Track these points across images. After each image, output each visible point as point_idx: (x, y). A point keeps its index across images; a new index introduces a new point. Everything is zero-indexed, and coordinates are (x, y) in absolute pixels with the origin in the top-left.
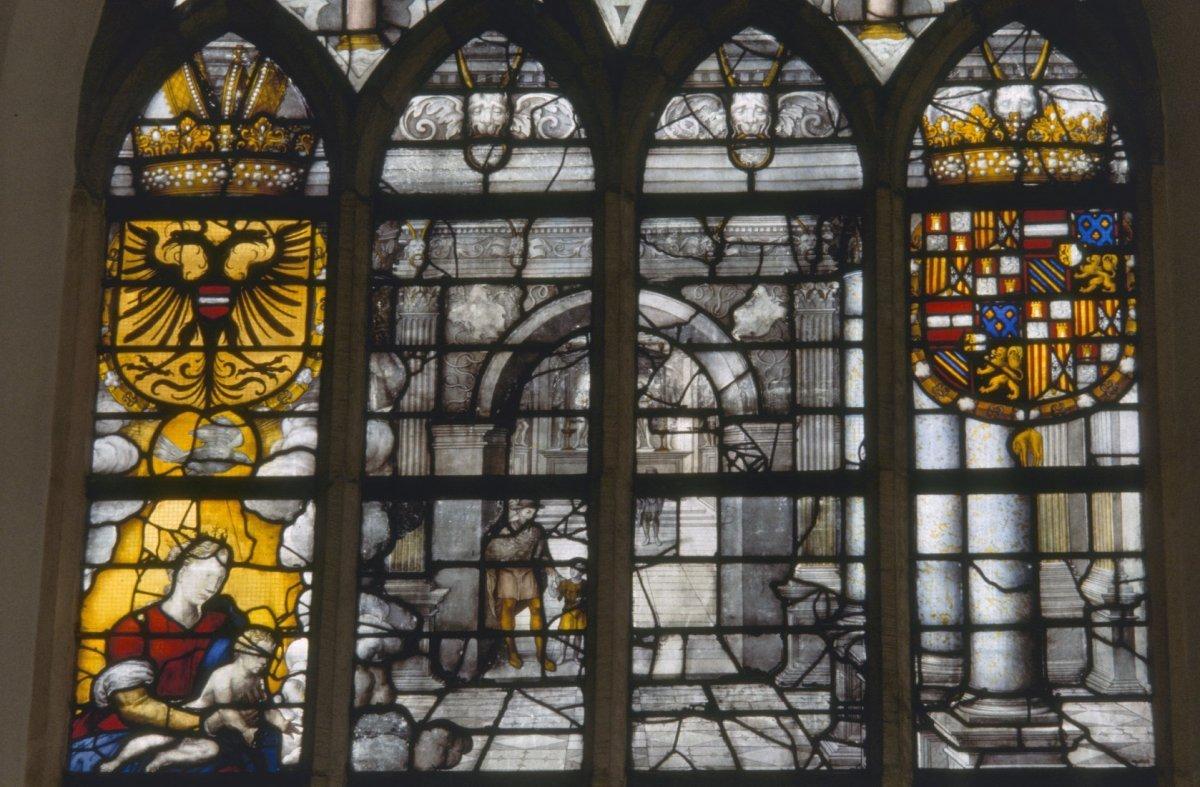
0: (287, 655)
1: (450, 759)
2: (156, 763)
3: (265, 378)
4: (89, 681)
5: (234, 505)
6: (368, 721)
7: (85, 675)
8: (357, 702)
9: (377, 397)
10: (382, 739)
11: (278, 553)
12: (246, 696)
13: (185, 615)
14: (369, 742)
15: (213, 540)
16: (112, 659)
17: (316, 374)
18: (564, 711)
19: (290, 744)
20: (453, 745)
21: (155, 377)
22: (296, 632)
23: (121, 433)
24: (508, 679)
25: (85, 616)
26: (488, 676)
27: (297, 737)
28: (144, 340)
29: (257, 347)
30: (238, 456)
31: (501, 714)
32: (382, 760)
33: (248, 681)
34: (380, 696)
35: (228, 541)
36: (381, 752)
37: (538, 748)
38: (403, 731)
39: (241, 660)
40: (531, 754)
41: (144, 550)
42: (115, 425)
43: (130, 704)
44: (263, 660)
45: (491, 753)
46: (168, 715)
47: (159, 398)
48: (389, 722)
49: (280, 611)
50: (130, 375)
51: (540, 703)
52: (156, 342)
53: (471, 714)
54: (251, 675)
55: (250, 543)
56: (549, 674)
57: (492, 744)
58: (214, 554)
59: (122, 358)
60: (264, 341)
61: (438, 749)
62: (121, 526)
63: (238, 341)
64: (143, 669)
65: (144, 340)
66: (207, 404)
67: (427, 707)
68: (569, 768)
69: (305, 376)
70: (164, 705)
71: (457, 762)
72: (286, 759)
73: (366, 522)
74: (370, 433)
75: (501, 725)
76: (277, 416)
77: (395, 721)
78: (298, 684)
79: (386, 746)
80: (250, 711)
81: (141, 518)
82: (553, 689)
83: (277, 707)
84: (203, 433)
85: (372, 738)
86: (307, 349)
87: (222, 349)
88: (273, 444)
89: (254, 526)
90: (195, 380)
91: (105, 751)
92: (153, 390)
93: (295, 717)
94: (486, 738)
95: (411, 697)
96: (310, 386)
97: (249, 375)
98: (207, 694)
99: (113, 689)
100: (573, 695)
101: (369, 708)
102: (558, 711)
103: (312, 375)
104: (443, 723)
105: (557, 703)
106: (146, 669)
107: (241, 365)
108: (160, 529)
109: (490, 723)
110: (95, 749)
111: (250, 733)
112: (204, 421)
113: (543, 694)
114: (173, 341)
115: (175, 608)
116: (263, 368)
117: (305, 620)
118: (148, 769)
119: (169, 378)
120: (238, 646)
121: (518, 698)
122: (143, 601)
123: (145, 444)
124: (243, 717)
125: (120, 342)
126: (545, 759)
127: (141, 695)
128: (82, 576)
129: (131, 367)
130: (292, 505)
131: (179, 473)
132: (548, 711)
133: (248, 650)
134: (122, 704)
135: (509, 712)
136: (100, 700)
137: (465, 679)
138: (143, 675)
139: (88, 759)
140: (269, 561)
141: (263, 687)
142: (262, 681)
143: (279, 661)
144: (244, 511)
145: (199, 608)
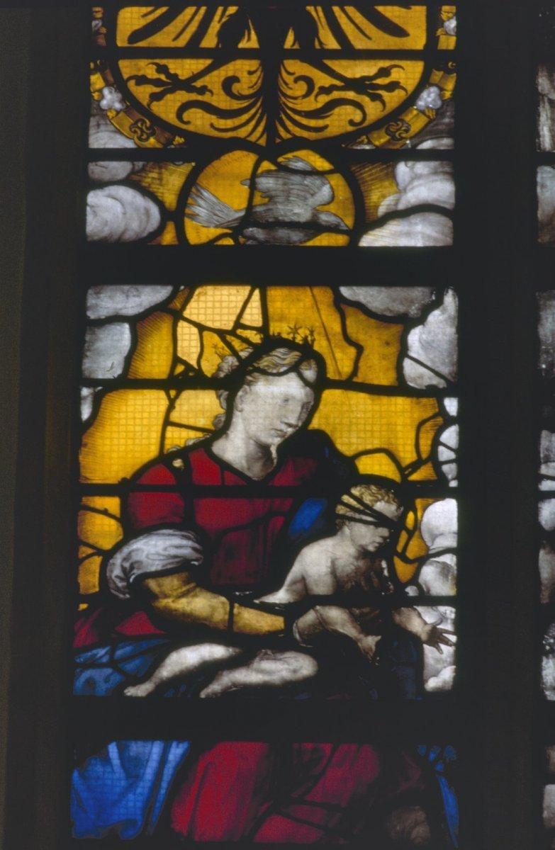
0: (423, 527)
2: (215, 687)
3: (365, 100)
4: (97, 560)
5: (323, 295)
7: (90, 551)
9: (551, 131)
11: (399, 369)
12: (358, 584)
13: (250, 459)
15: (290, 345)
16: (132, 527)
17: (448, 94)
19: (438, 661)
21: (182, 97)
22: (437, 490)
23: (131, 182)
25: (85, 460)
27: (448, 651)
28: (162, 39)
29: (348, 52)
30: (324, 218)
33: (361, 563)
35: (316, 347)
39: (346, 530)
41: (176, 360)
42: (121, 168)
43: (166, 596)
44: (384, 532)
46: (231, 614)
47: (191, 128)
49: (408, 456)
50: (142, 93)
52: (182, 42)
54: (363, 553)
55: (352, 351)
58: (295, 368)
59: (127, 68)
60: (359, 43)
62: (139, 323)
63: (317, 43)
64: (185, 542)
65: (162, 39)
66: (270, 140)
69: (429, 98)
70: (223, 599)
72: (432, 684)
73: (544, 321)
74: (543, 186)
76: (388, 158)
78: (445, 568)
80: (366, 610)
81: (171, 311)
83: (412, 603)
84: (266, 183)
86: (431, 57)
87: (292, 54)
88: (382, 200)
89: (356, 325)
90: (245, 104)
91: (130, 666)
92: (179, 115)
93: (443, 619)
96: (440, 112)
97: (336, 95)
98: (294, 583)
99: (136, 572)
103: (441, 96)
106: (190, 543)
107: (323, 80)
108: (201, 328)
110: (113, 663)
111: (370, 641)
112: (266, 165)
114: (210, 41)
115: (234, 449)
116: (361, 85)
117: (450, 470)
118: (203, 695)
119: (206, 98)
120: (341, 510)
122: (178, 438)
123: (170, 199)
124: (355, 619)
125: (122, 41)
127: (186, 582)
128: (78, 400)
129: (141, 80)
130: (418, 294)
131: (229, 242)
133: (357, 516)
134: (155, 597)
136: (118, 589)
138: (187, 552)
139: (102, 678)
140: (385, 378)
141: (386, 573)
142: (384, 564)
143: (411, 534)
144: (340, 304)
145: (273, 450)
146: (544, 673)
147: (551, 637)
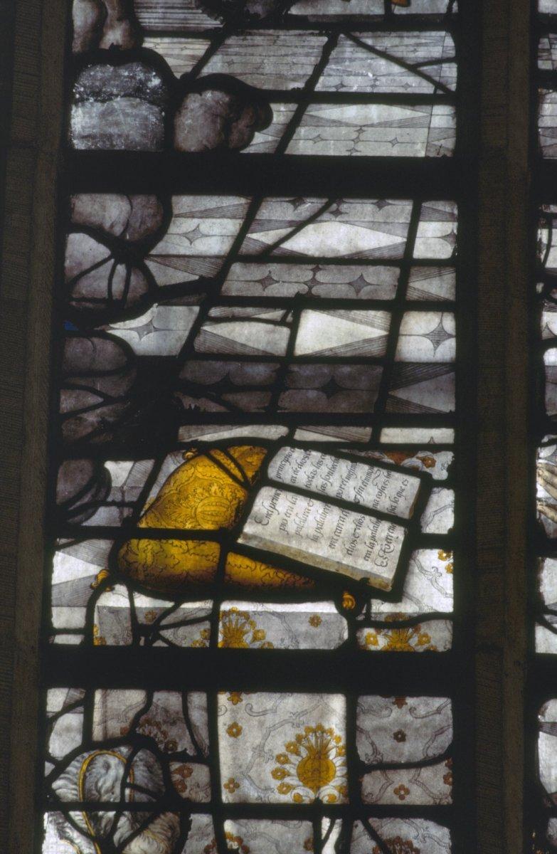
1: (235, 136)
6: (98, 74)
8: (77, 46)
10: (119, 103)
14: (99, 107)
18: (425, 69)
20: (238, 119)
24: (327, 16)
26: (294, 11)
31: (319, 70)
32: (120, 136)
34: (114, 36)
36: (117, 124)
37: (380, 125)
38: (154, 90)
40: (369, 134)
45: (302, 131)
48: (133, 77)
51: (384, 55)
53: (268, 68)
56: (398, 10)
57: (304, 117)
61: (214, 122)
67: (193, 57)
68: (432, 155)
71: (247, 142)
75: (319, 87)
77: (141, 76)
79: (126, 115)
82: (405, 34)
85: (103, 101)
94: (293, 107)
95: (166, 40)
100: (438, 44)
101: (96, 54)
102: (414, 68)
104: (218, 82)
105: (412, 55)
109: (300, 85)
113: (388, 42)
121: (347, 49)
126: (394, 142)
132: (396, 69)
135: (331, 67)
137: (257, 15)
146: (73, 121)
147: (82, 86)
